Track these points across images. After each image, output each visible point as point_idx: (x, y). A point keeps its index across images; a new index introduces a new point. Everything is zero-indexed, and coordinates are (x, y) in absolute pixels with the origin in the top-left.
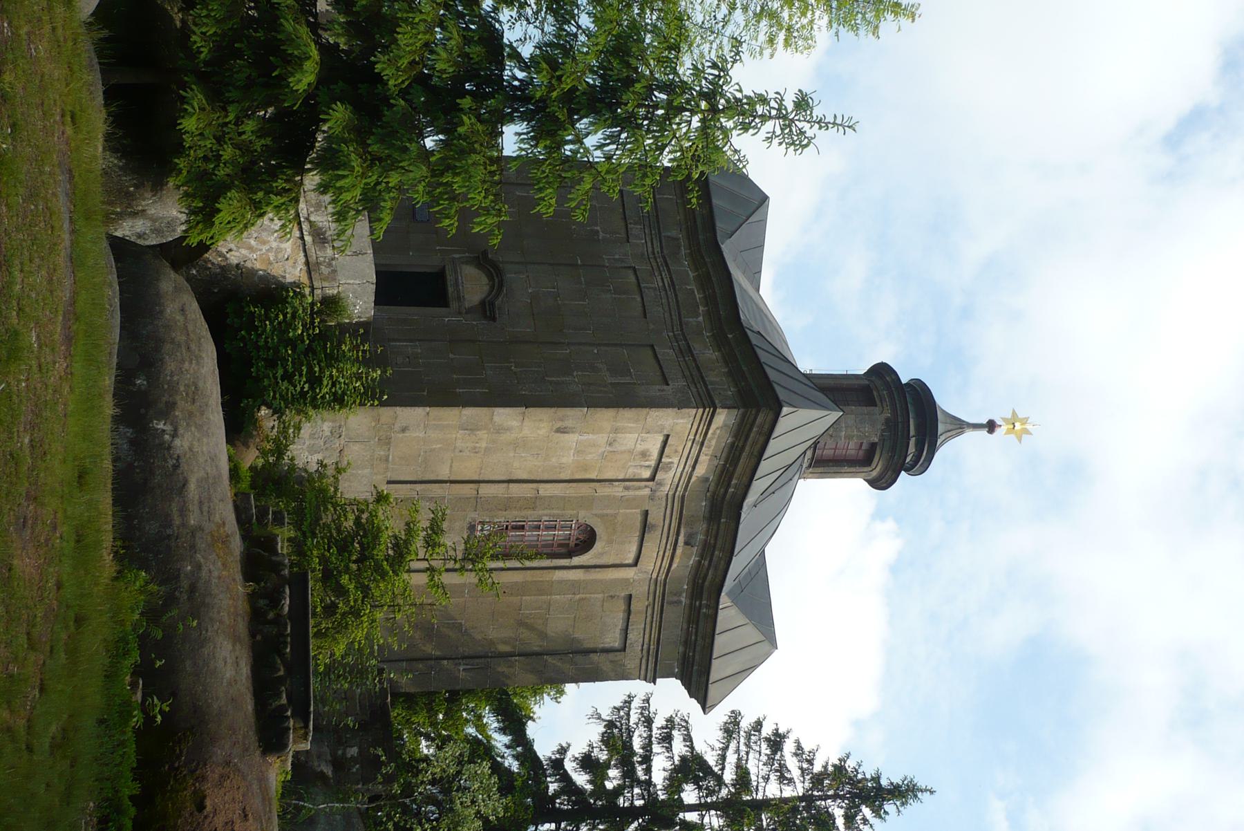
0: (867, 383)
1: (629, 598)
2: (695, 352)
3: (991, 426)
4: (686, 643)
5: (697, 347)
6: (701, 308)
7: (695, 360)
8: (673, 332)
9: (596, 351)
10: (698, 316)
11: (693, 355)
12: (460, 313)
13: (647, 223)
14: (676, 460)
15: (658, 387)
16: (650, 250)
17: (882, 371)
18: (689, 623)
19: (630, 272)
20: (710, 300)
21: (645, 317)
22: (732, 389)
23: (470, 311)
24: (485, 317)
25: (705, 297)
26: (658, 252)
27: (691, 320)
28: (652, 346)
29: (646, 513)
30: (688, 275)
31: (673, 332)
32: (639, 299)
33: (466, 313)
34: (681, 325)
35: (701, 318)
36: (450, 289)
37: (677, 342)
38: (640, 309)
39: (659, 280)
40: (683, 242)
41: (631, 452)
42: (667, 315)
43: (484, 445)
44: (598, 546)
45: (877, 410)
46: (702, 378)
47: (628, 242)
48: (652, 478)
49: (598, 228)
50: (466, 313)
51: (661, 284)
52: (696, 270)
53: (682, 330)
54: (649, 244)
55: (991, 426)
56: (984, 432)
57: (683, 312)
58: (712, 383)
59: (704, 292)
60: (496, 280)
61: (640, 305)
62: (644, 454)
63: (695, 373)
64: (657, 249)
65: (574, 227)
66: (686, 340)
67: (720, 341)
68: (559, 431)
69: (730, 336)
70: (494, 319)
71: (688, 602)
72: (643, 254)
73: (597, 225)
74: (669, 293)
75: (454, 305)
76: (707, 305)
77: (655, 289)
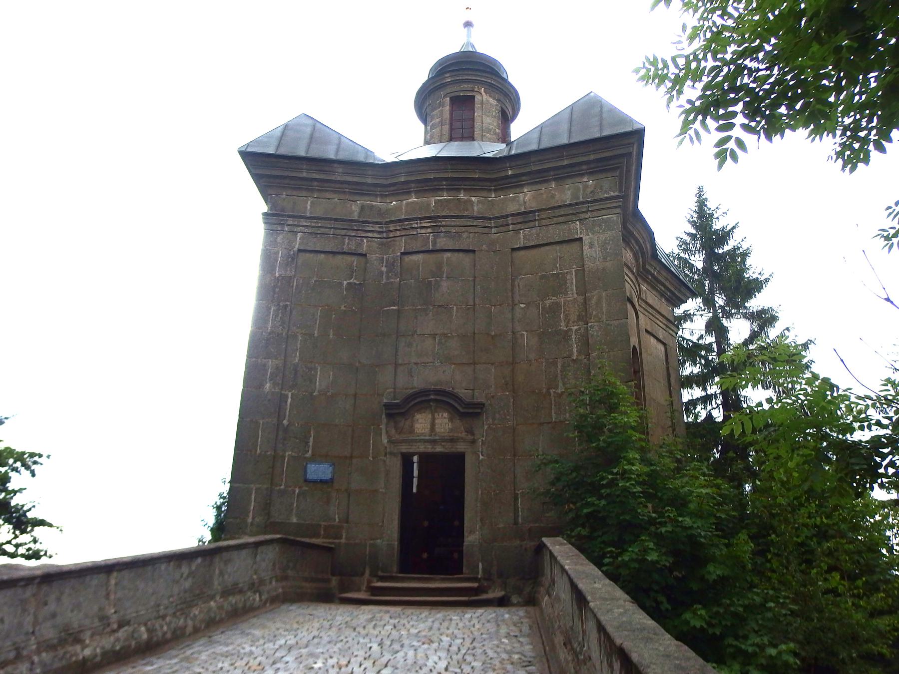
0: (448, 99)
2: (523, 210)
5: (512, 208)
6: (462, 196)
7: (539, 211)
8: (491, 228)
9: (522, 306)
10: (471, 201)
11: (534, 212)
12: (473, 442)
13: (343, 232)
15: (586, 248)
16: (376, 235)
18: (654, 288)
19: (407, 258)
21: (474, 251)
22: (585, 180)
23: (470, 432)
24: (478, 415)
25: (448, 190)
26: (380, 228)
27: (476, 208)
28: (513, 250)
30: (414, 202)
31: (491, 228)
32: (449, 254)
33: (473, 434)
34: (485, 218)
35: (473, 199)
36: (439, 449)
37: (508, 225)
38: (461, 255)
39: (423, 231)
42: (472, 230)
45: (478, 98)
47: (365, 255)
49: (345, 283)
50: (473, 434)
51: (429, 230)
52: (409, 193)
53: (490, 219)
54: (370, 235)
57: (466, 214)
59: (442, 190)
60: (432, 397)
61: (456, 254)
64: (377, 228)
65: (343, 308)
66: (507, 216)
70: (481, 406)
72: (382, 244)
73: (341, 284)
74: (444, 223)
75: (461, 447)
76: (458, 190)
77: (435, 237)
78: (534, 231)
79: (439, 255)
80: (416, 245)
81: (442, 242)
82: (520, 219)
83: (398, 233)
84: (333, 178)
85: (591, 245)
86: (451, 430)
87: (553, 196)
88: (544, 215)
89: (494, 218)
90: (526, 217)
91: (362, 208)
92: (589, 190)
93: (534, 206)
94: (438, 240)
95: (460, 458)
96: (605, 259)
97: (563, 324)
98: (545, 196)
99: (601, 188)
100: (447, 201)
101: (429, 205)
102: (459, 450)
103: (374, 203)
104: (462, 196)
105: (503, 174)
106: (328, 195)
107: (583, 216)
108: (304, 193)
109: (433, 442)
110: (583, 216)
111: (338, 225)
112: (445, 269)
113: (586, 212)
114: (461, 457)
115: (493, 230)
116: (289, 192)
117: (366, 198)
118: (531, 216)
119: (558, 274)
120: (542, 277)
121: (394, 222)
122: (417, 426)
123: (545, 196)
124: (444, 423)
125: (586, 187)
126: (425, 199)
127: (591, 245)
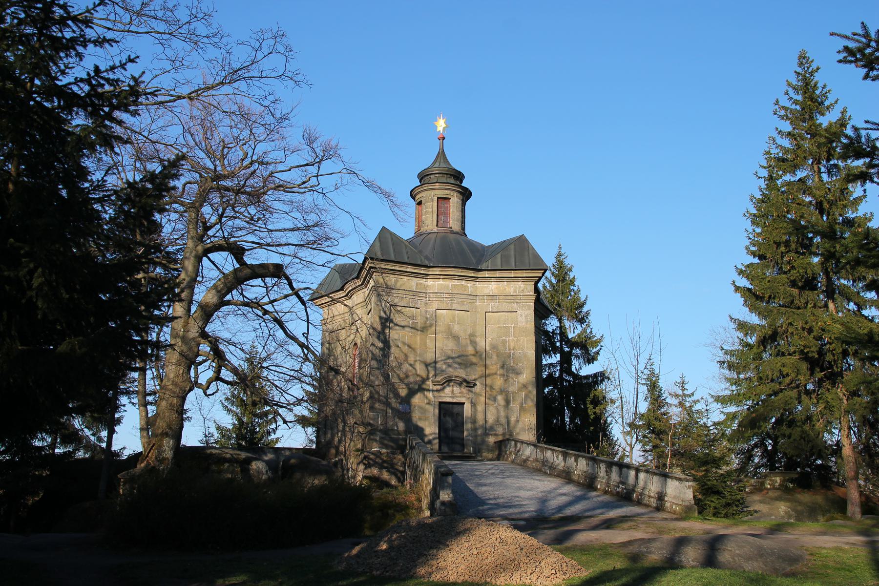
2: (491, 294)
5: (486, 292)
13: (409, 297)
16: (424, 299)
39: (446, 299)
40: (419, 280)
54: (421, 298)
57: (465, 293)
58: (515, 291)
63: (509, 297)
78: (496, 305)
80: (444, 307)
81: (455, 306)
82: (490, 298)
83: (434, 299)
85: (521, 316)
87: (505, 289)
88: (501, 298)
90: (493, 297)
91: (417, 284)
93: (496, 292)
94: (454, 305)
96: (527, 323)
97: (507, 350)
99: (527, 289)
100: (457, 285)
101: (449, 286)
104: (464, 283)
107: (518, 301)
110: (518, 301)
111: (407, 293)
119: (506, 327)
120: (499, 327)
126: (447, 283)
127: (521, 316)
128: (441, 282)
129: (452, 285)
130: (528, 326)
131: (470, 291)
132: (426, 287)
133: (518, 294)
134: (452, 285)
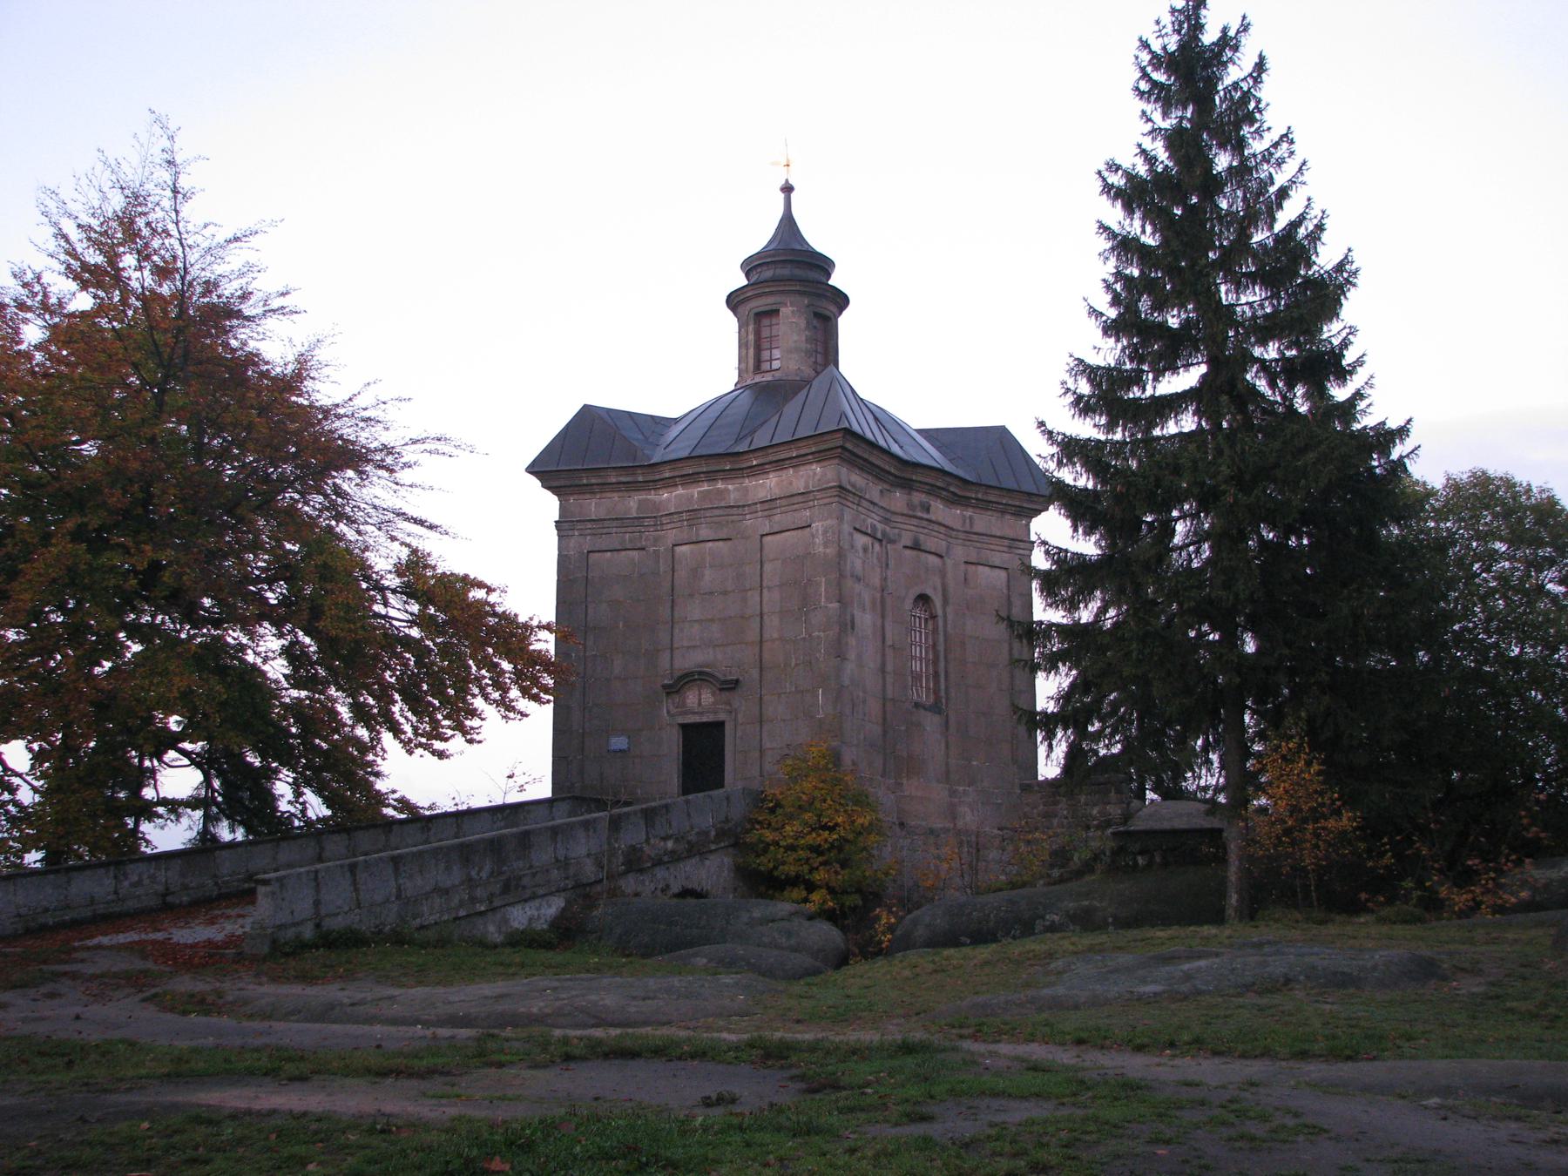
1: (966, 562)
3: (788, 189)
4: (1003, 512)
5: (762, 495)
10: (727, 490)
11: (776, 499)
14: (869, 520)
17: (735, 301)
20: (711, 476)
27: (732, 497)
28: (762, 536)
29: (905, 547)
30: (681, 495)
32: (710, 544)
35: (730, 487)
38: (721, 543)
40: (643, 496)
41: (864, 562)
43: (861, 694)
44: (929, 592)
46: (803, 493)
48: (880, 541)
53: (744, 506)
55: (788, 189)
56: (793, 195)
57: (723, 504)
58: (807, 483)
62: (865, 550)
63: (795, 500)
66: (756, 504)
67: (760, 470)
68: (853, 628)
69: (755, 463)
71: (971, 510)
75: (722, 717)
79: (702, 545)
81: (705, 533)
82: (766, 506)
84: (609, 481)
86: (714, 703)
87: (791, 484)
89: (749, 505)
90: (769, 504)
92: (817, 478)
93: (777, 492)
95: (720, 725)
98: (785, 483)
101: (693, 496)
102: (721, 719)
103: (649, 497)
104: (720, 485)
105: (749, 464)
106: (609, 495)
108: (588, 496)
109: (701, 714)
112: (708, 558)
113: (813, 500)
114: (720, 725)
115: (748, 517)
116: (576, 497)
117: (643, 492)
118: (773, 505)
121: (666, 515)
122: (688, 701)
123: (785, 483)
124: (707, 697)
125: (815, 474)
128: (680, 491)
129: (699, 492)
130: (828, 551)
131: (733, 498)
132: (656, 506)
133: (811, 489)
134: (699, 492)
